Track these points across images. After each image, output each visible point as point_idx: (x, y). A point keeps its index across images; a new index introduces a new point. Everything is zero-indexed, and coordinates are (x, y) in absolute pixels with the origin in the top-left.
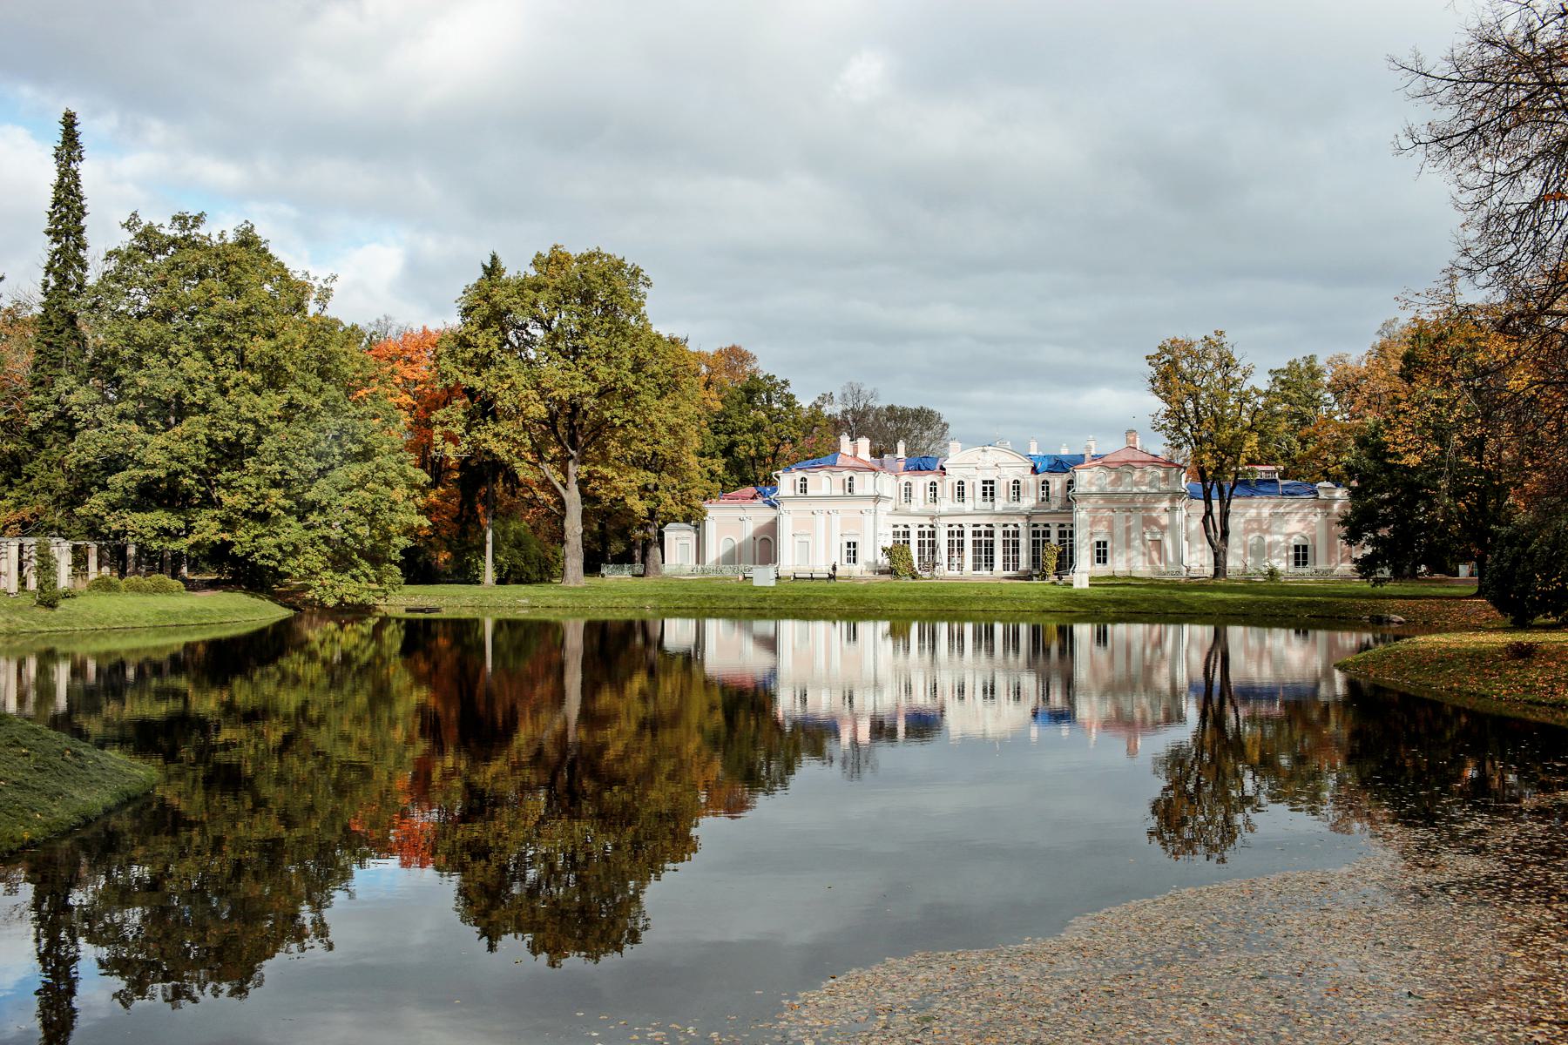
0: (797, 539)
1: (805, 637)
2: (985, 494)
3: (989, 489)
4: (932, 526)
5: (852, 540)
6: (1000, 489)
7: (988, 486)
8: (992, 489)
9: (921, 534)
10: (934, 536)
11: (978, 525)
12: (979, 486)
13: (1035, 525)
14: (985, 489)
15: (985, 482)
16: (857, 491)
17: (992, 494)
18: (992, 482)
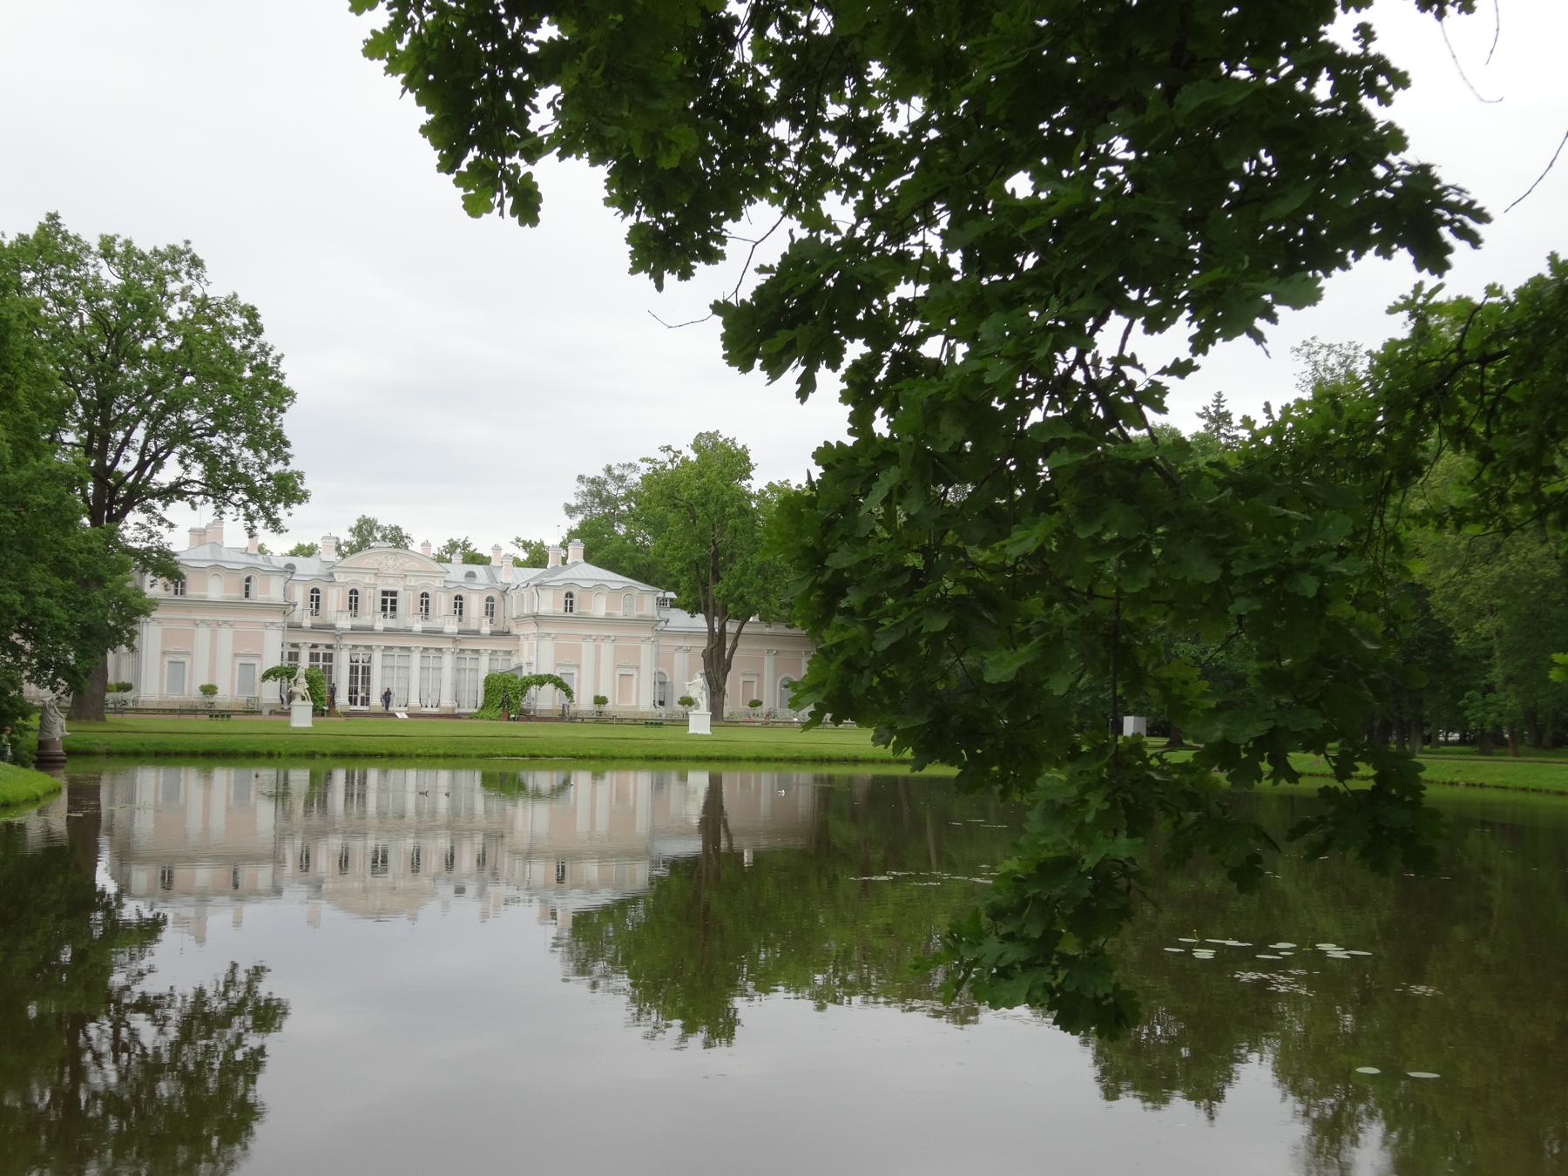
0: (168, 658)
1: (172, 793)
2: (384, 609)
3: (389, 602)
4: (329, 647)
5: (252, 661)
6: (408, 602)
7: (389, 598)
8: (394, 602)
9: (314, 657)
10: (331, 661)
11: (392, 648)
12: (379, 597)
13: (462, 651)
14: (384, 601)
15: (385, 593)
16: (258, 595)
17: (393, 609)
18: (394, 593)
